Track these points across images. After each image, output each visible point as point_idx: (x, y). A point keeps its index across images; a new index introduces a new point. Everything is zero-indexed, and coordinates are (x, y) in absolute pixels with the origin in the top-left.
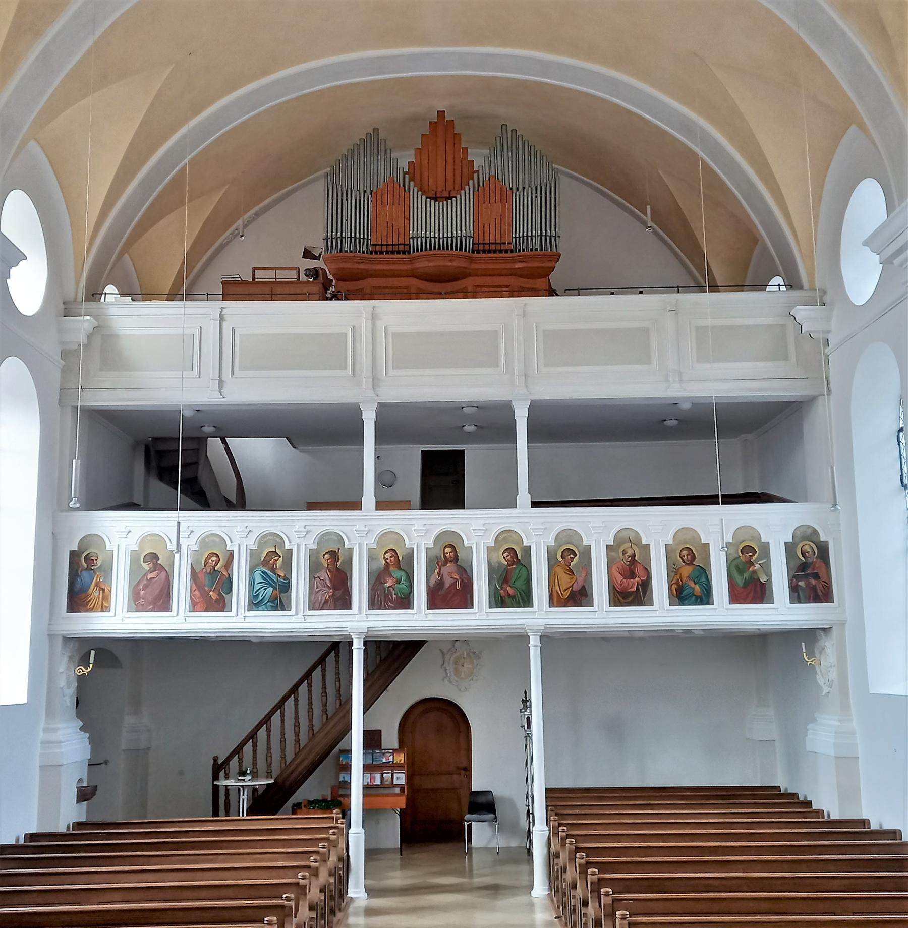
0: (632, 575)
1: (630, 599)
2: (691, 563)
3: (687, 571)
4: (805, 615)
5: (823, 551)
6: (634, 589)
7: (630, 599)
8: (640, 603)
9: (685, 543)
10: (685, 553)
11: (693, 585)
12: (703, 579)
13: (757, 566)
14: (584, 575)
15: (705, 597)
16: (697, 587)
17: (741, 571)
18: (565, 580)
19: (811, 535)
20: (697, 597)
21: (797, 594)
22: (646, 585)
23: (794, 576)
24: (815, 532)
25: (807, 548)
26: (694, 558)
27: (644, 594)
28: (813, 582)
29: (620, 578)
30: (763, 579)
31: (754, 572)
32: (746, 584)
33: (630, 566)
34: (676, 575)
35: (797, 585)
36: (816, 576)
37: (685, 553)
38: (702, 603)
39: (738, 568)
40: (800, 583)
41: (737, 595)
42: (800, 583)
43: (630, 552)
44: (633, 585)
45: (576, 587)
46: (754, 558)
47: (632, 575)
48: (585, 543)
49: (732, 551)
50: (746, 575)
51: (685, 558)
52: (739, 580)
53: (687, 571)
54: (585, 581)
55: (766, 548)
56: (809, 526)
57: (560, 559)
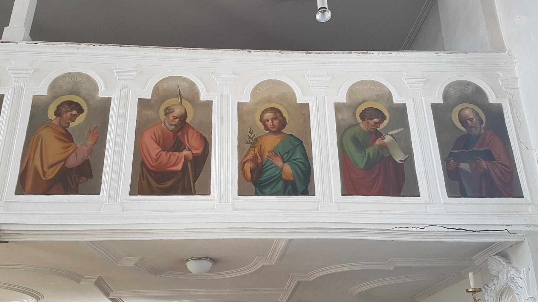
0: (178, 146)
1: (170, 183)
2: (278, 131)
3: (271, 142)
4: (479, 214)
5: (495, 117)
6: (179, 167)
7: (170, 183)
8: (188, 191)
9: (269, 101)
10: (269, 115)
11: (280, 164)
12: (298, 155)
13: (388, 139)
14: (90, 143)
15: (301, 184)
16: (287, 169)
17: (360, 144)
18: (54, 150)
19: (472, 95)
20: (287, 183)
21: (459, 184)
22: (201, 162)
23: (451, 155)
24: (479, 91)
25: (467, 112)
26: (283, 123)
27: (196, 177)
28: (484, 164)
29: (154, 149)
30: (399, 157)
31: (384, 147)
32: (370, 165)
33: (175, 132)
34: (253, 146)
35: (457, 168)
36: (489, 156)
37: (269, 115)
38: (294, 192)
39: (356, 141)
40: (462, 166)
41: (355, 182)
42: (462, 166)
43: (178, 111)
44: (177, 161)
45: (72, 162)
46: (382, 126)
47: (178, 146)
48: (102, 93)
49: (346, 115)
50: (370, 151)
51: (269, 123)
52: (359, 160)
53: (271, 142)
54: (90, 152)
55: (400, 113)
56: (469, 84)
57: (51, 115)
